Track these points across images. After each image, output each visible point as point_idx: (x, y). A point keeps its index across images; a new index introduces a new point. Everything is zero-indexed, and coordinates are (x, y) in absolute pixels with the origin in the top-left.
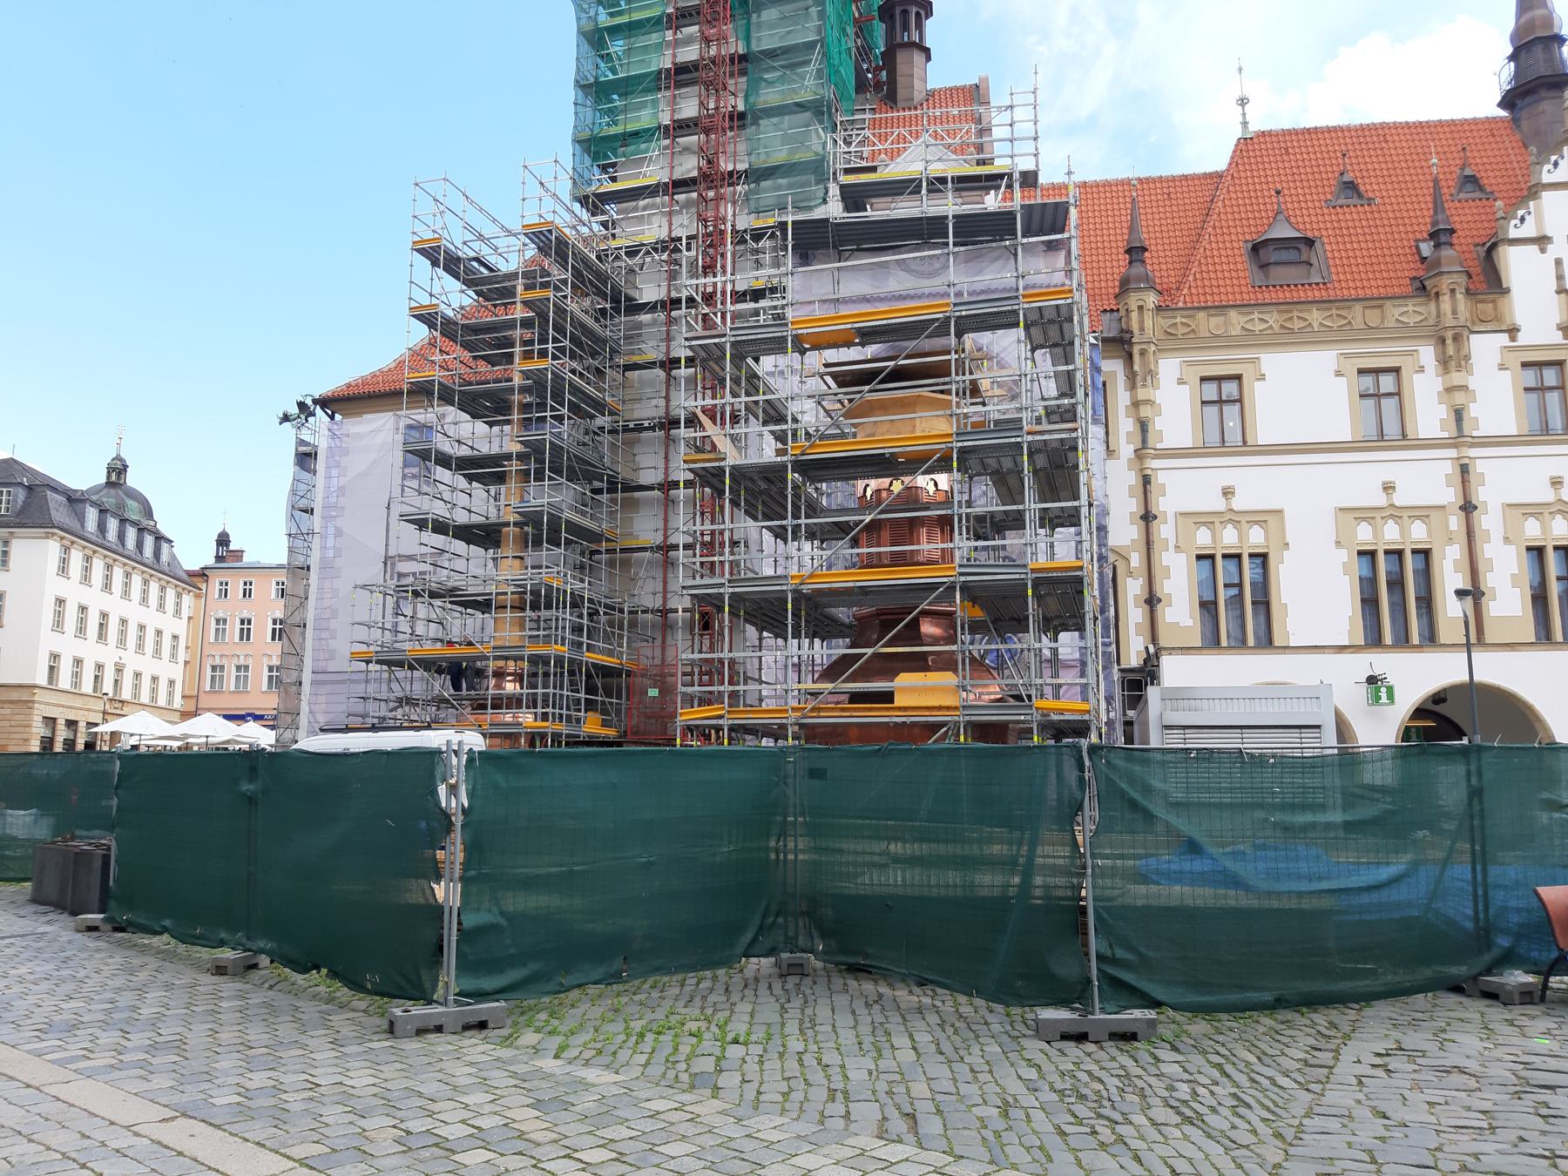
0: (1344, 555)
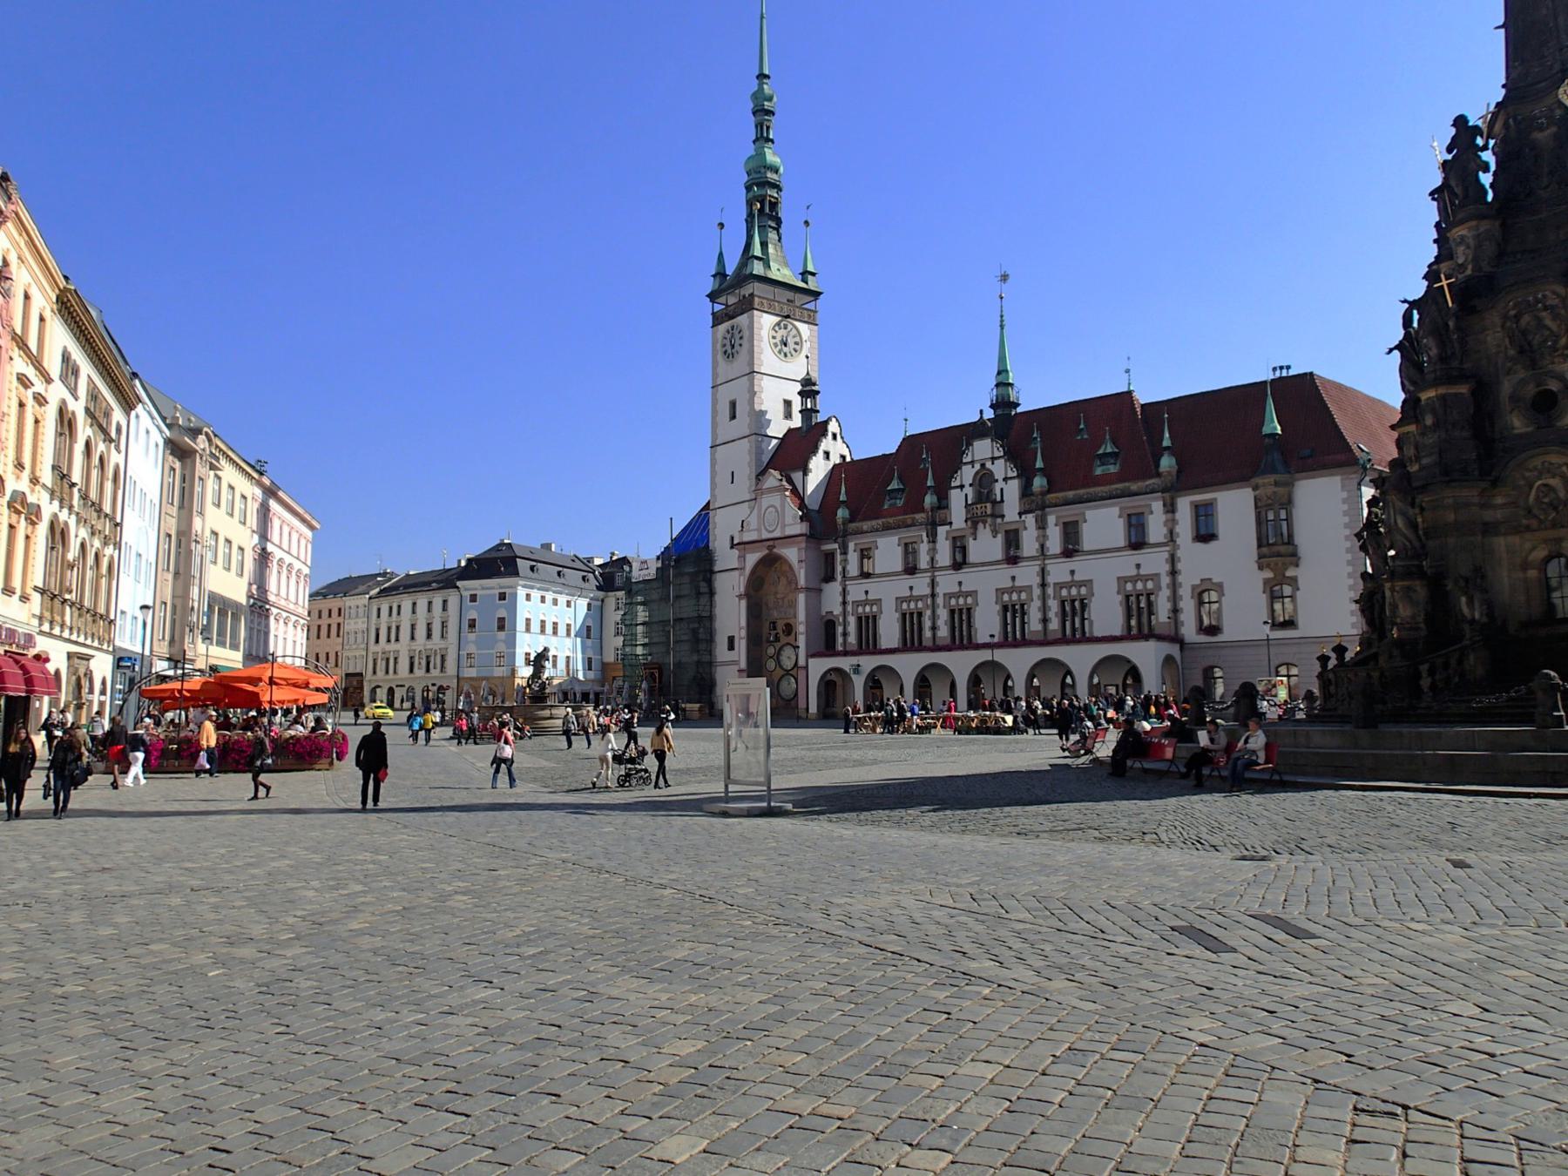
0: (897, 615)
